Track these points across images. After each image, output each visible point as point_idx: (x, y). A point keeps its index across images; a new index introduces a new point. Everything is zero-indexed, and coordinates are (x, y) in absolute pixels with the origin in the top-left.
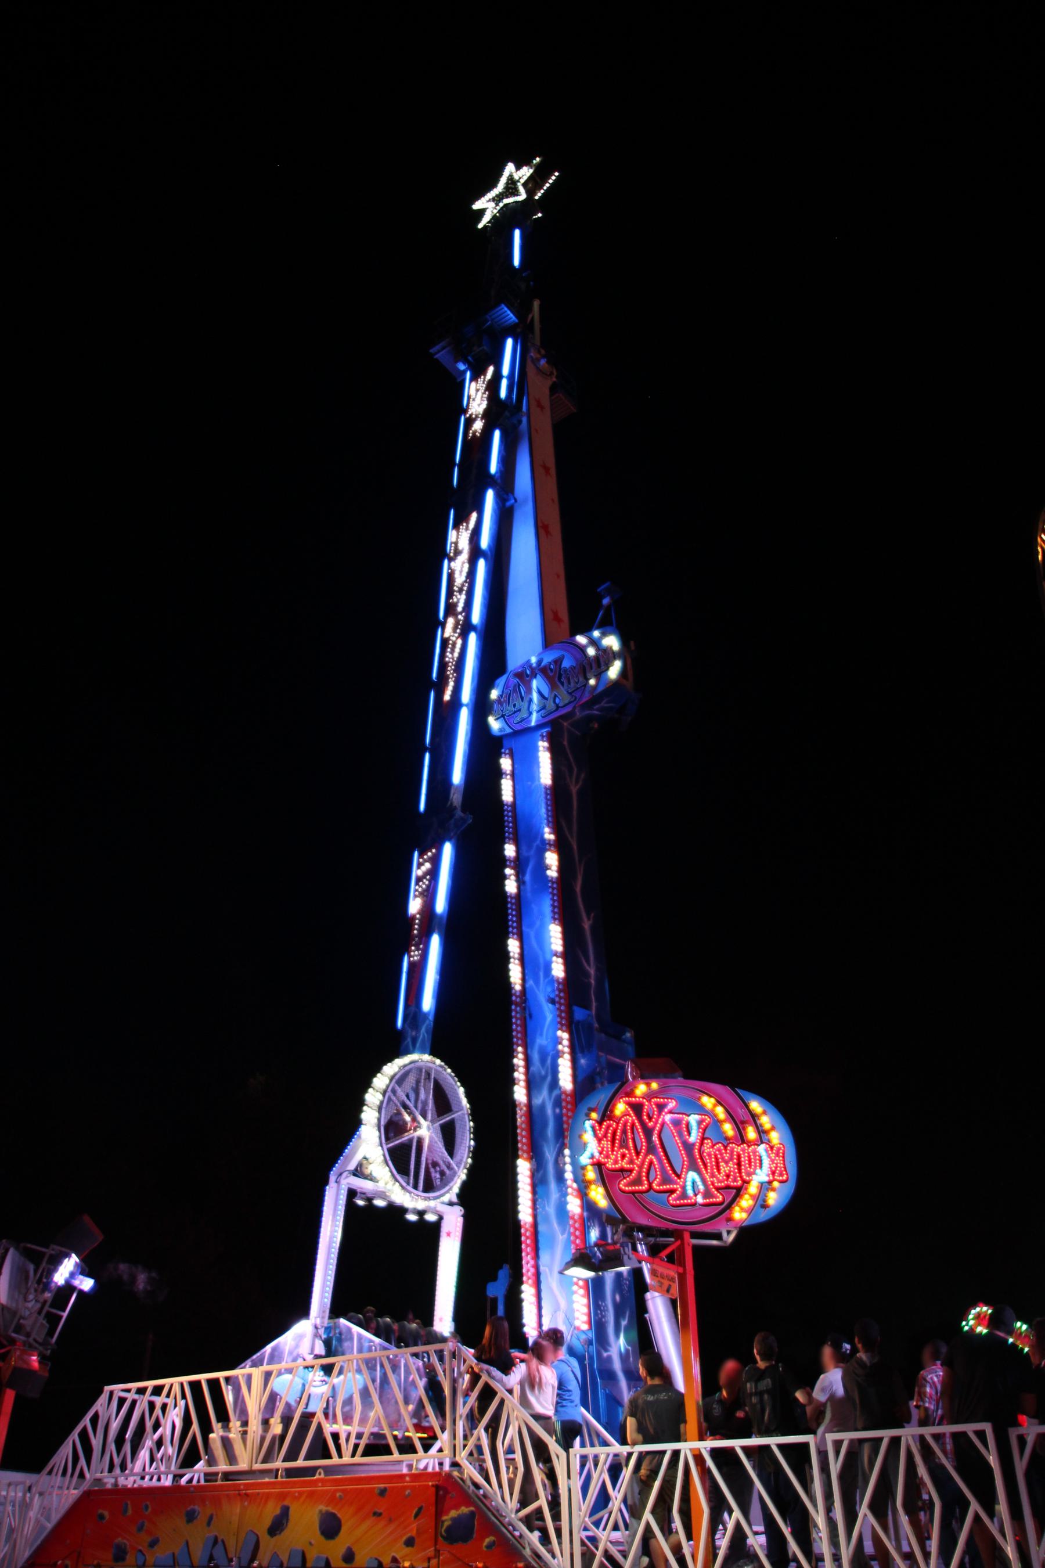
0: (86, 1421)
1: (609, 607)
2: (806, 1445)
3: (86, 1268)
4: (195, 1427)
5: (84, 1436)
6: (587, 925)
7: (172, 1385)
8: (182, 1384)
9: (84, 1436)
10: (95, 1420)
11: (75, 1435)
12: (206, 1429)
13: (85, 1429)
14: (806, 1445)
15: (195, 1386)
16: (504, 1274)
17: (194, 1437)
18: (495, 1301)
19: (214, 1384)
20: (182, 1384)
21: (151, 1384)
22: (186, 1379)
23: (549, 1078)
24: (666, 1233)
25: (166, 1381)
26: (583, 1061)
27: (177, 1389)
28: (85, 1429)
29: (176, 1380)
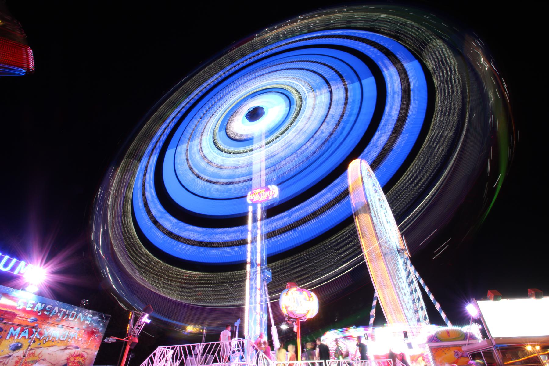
0: (152, 355)
1: (275, 180)
2: (322, 362)
3: (149, 318)
4: (183, 356)
5: (151, 357)
6: (264, 246)
7: (177, 347)
8: (180, 347)
9: (151, 358)
10: (154, 355)
11: (148, 358)
12: (186, 357)
13: (151, 356)
14: (322, 362)
15: (184, 347)
16: (239, 321)
17: (183, 358)
18: (236, 327)
19: (189, 347)
20: (180, 347)
21: (171, 346)
22: (181, 346)
23: (254, 279)
24: (295, 319)
25: (176, 346)
26: (262, 276)
27: (178, 347)
28: (151, 356)
29: (178, 346)
